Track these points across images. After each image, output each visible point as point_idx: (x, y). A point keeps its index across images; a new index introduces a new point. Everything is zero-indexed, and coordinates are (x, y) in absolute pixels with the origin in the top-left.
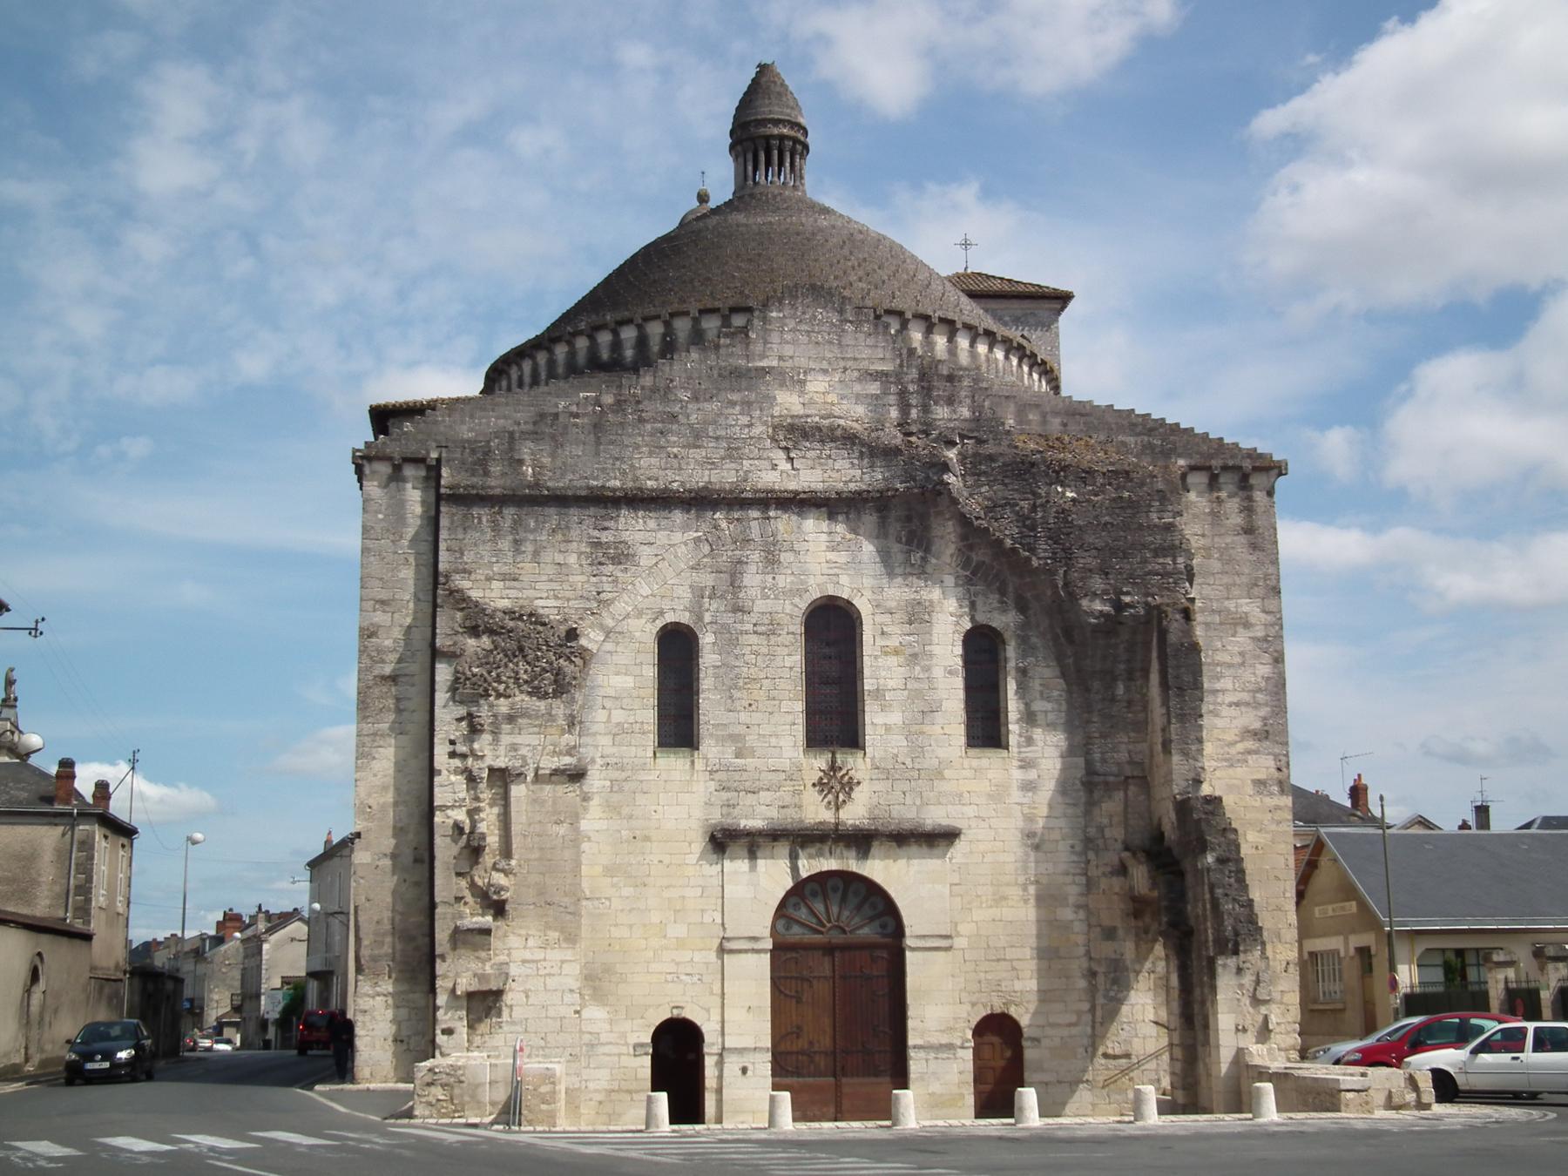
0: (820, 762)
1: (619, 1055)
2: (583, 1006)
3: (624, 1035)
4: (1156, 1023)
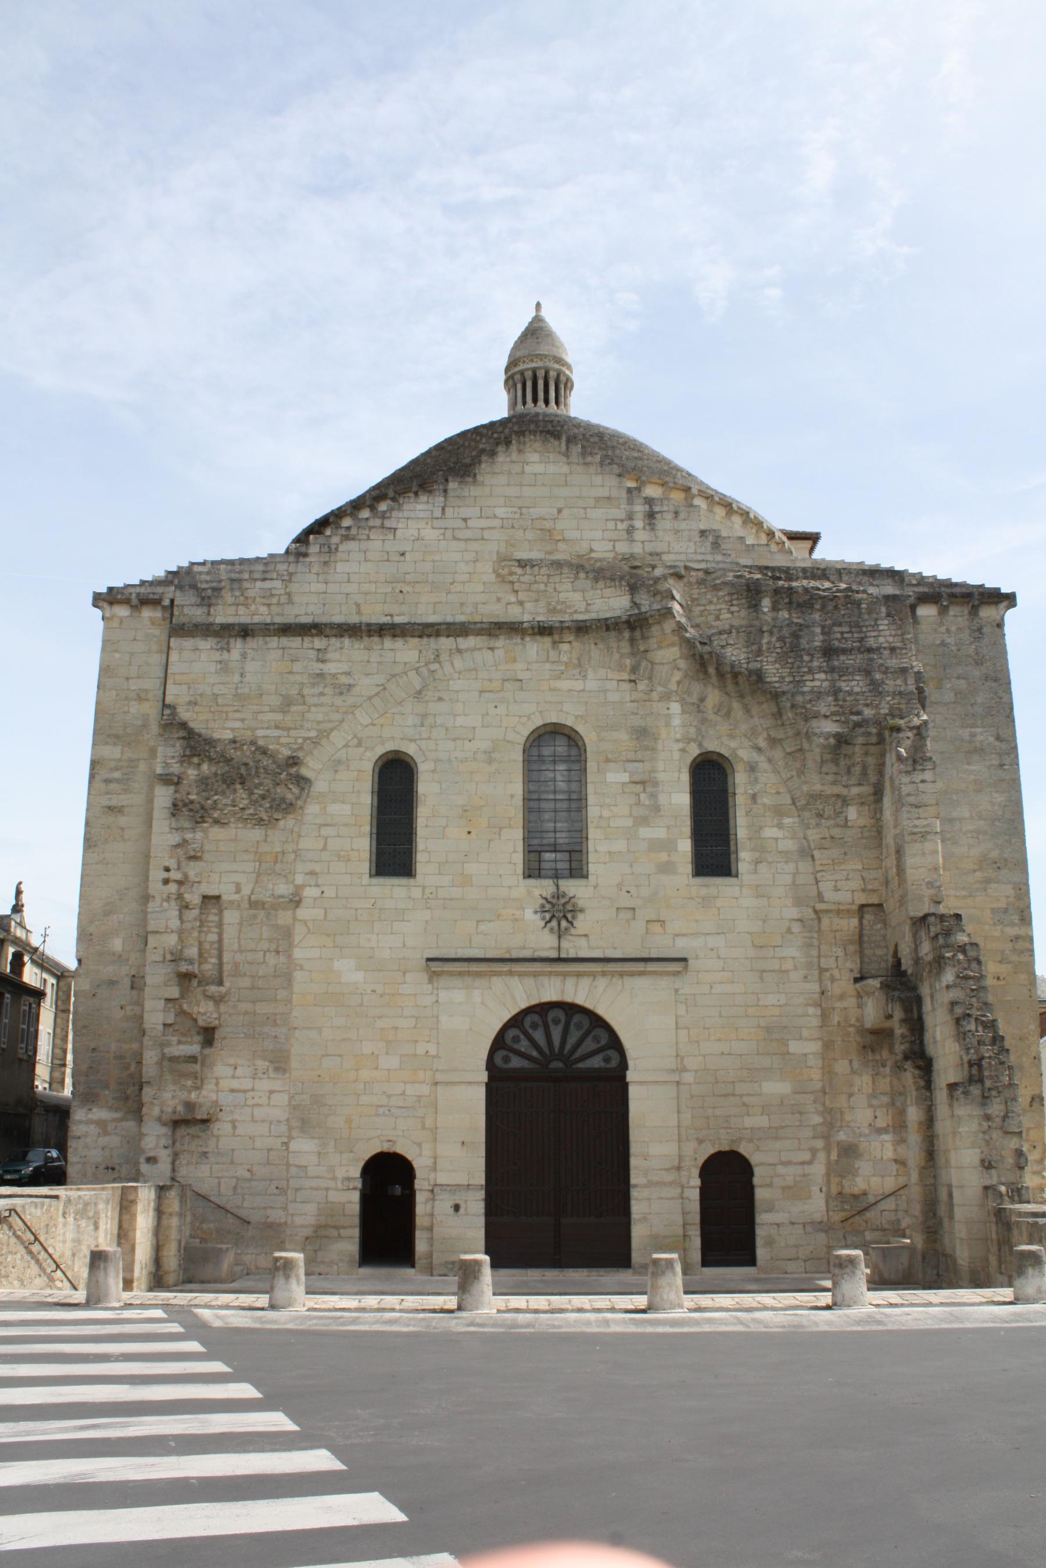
0: (544, 887)
1: (327, 1189)
2: (290, 1138)
3: (331, 1169)
4: (896, 1161)
